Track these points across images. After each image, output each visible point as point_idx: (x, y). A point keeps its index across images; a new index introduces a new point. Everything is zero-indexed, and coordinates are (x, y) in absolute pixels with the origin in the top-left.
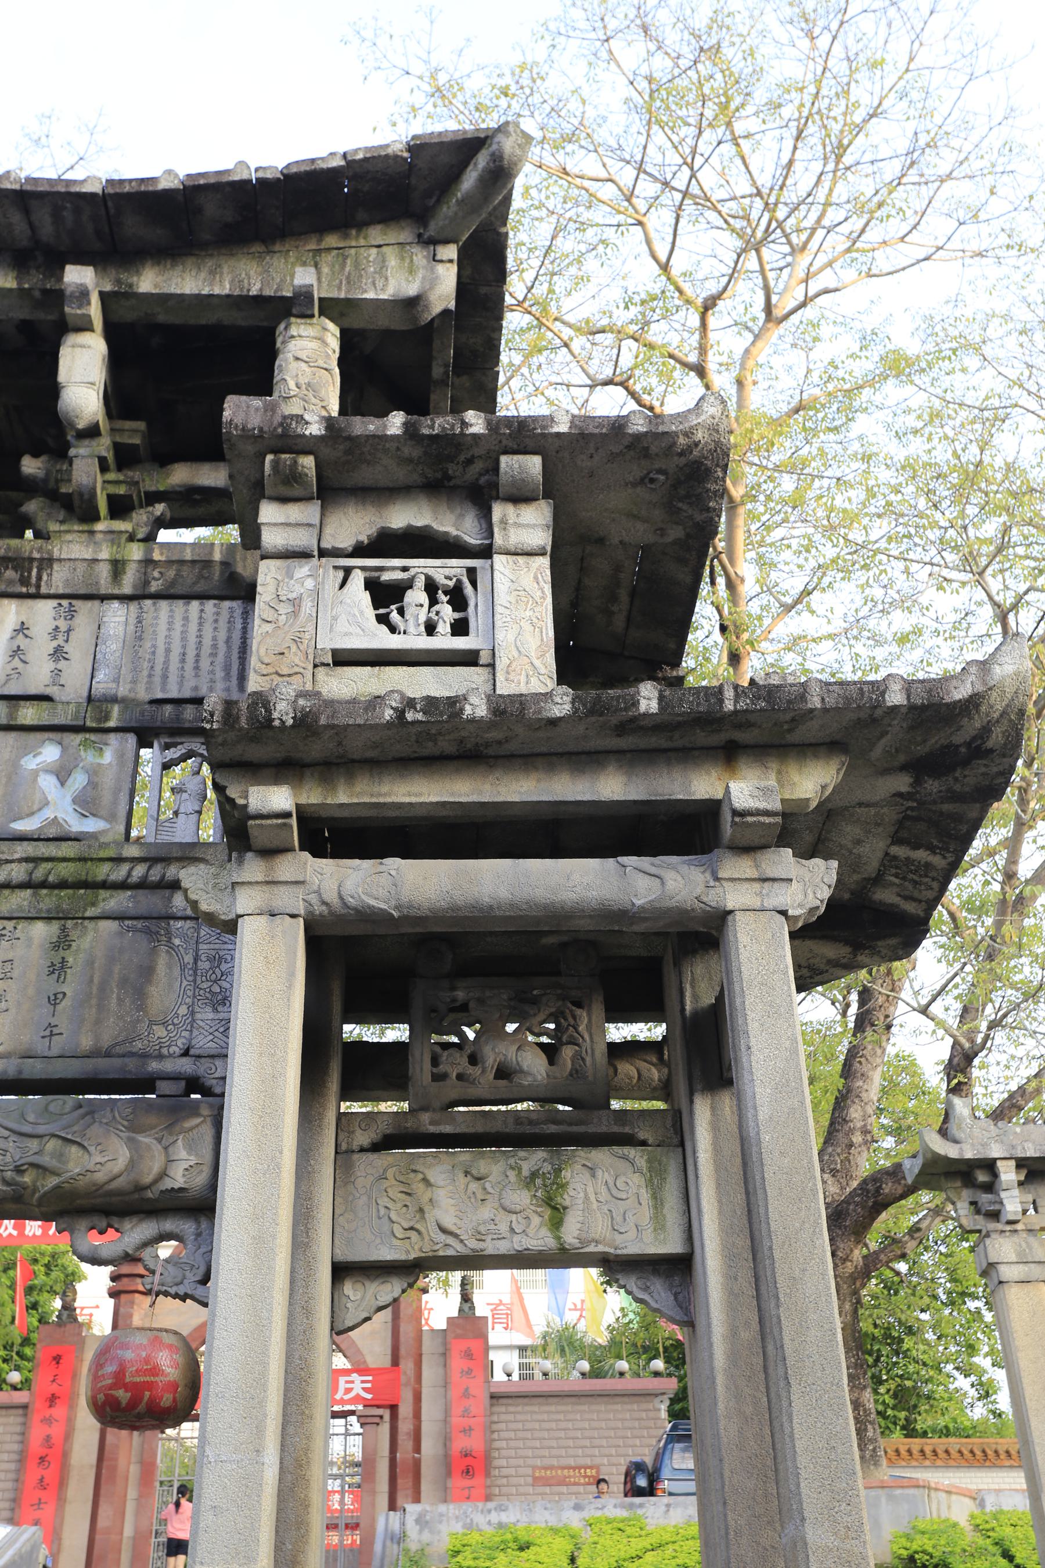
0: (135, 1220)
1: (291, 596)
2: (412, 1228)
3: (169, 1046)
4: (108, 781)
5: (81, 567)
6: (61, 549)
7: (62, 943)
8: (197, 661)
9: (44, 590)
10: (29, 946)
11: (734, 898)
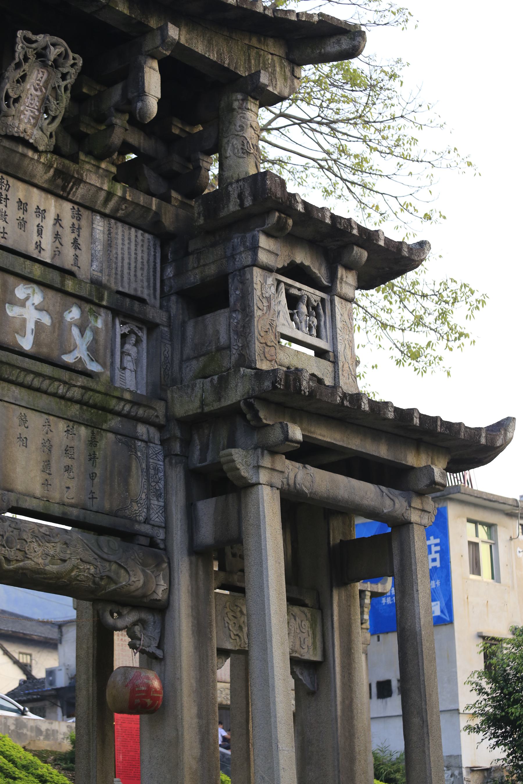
0: (128, 609)
1: (267, 295)
2: (237, 635)
3: (139, 516)
4: (102, 338)
5: (93, 189)
6: (86, 175)
7: (92, 442)
8: (135, 271)
9: (70, 197)
10: (80, 440)
11: (414, 517)
